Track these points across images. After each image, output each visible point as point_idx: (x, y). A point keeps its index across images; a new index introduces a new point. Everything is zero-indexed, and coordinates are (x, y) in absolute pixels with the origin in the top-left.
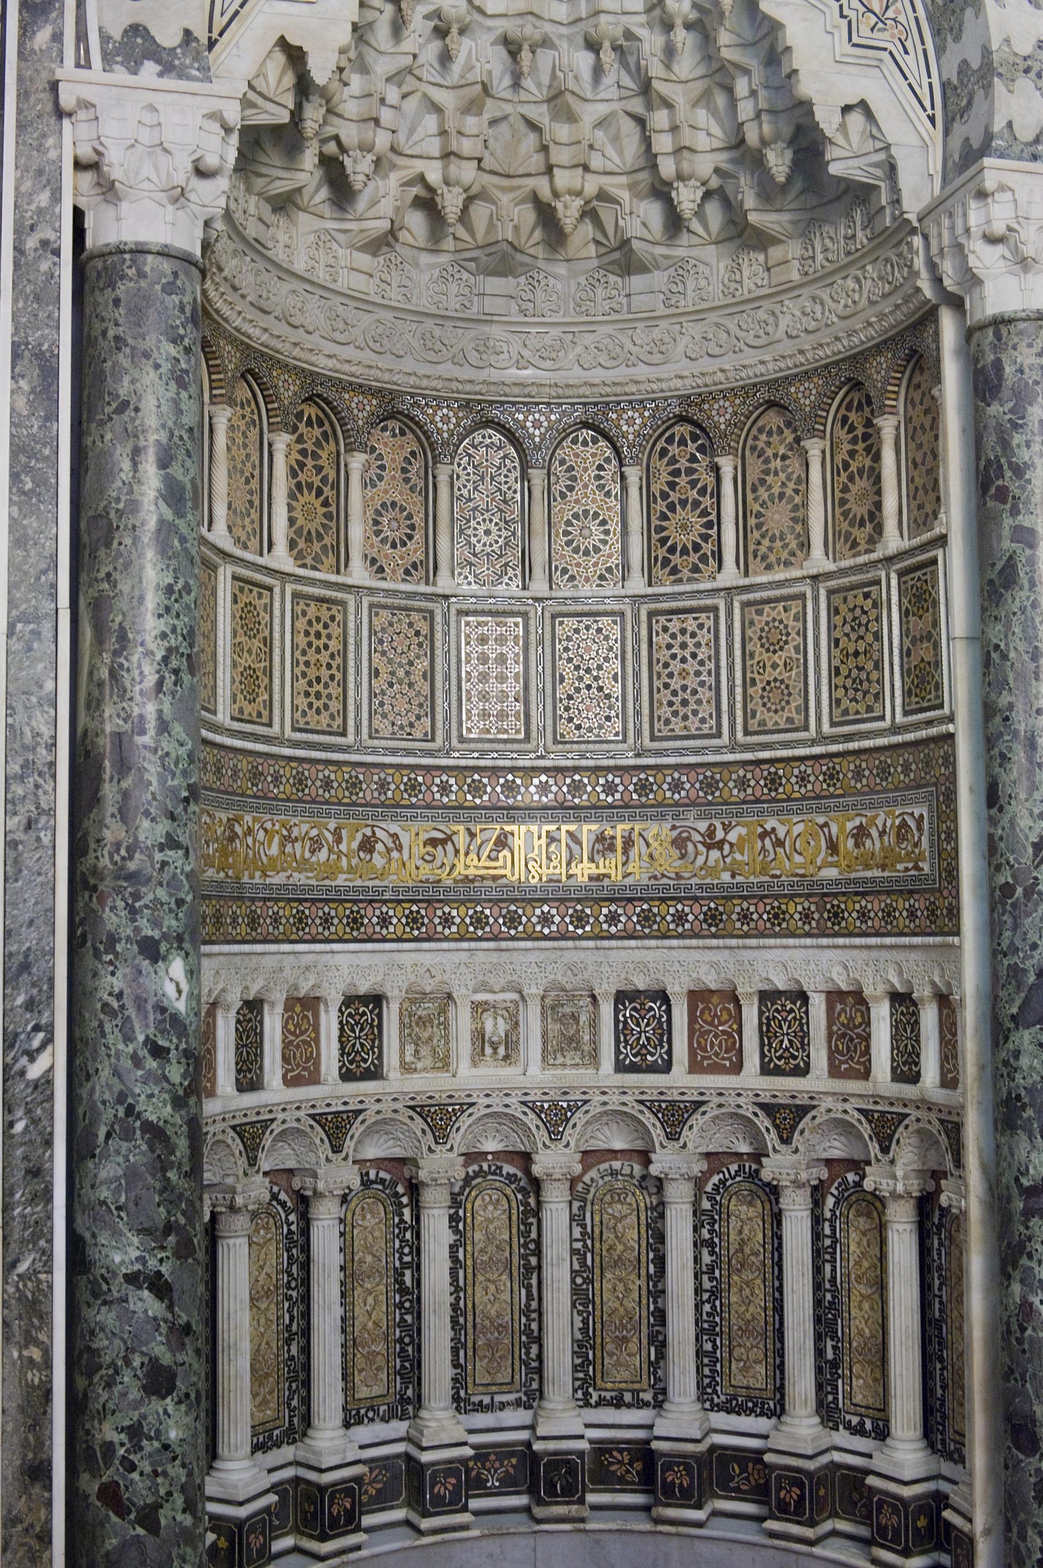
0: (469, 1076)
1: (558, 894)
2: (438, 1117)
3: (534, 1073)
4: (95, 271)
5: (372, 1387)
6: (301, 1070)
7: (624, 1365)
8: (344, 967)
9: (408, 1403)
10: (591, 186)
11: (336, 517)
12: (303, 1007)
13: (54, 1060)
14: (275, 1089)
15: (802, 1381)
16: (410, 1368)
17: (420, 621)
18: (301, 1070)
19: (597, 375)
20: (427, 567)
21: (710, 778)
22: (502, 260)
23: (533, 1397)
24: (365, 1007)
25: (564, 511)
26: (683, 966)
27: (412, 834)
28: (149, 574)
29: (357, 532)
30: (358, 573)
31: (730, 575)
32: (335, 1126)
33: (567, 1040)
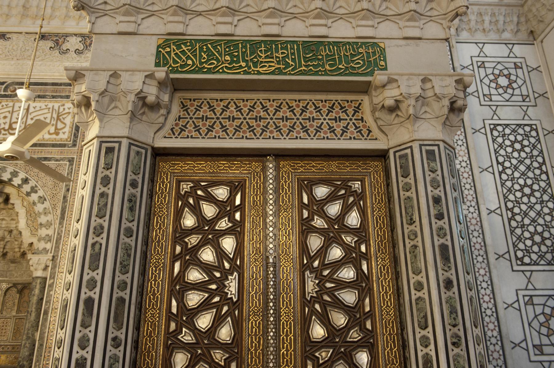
10: (22, 250)
19: (28, 278)
22: (13, 261)
25: (22, 301)
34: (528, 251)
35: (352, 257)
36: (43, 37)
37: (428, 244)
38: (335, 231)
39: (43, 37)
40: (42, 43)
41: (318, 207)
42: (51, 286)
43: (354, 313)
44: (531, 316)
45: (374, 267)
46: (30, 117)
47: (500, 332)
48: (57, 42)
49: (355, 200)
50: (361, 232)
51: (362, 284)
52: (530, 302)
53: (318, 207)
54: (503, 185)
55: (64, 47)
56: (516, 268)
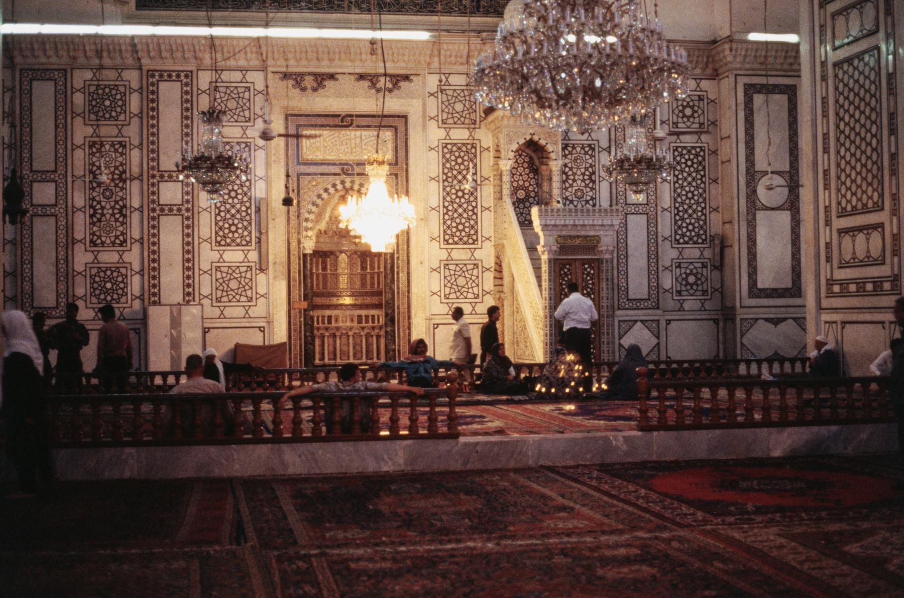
0: (341, 324)
1: (350, 305)
2: (338, 329)
3: (348, 324)
4: (305, 255)
5: (332, 357)
6: (323, 323)
7: (359, 356)
8: (328, 313)
9: (335, 359)
11: (326, 265)
12: (323, 317)
13: (302, 319)
14: (321, 325)
15: (375, 355)
16: (335, 355)
17: (336, 276)
18: (323, 323)
20: (336, 270)
21: (367, 293)
23: (348, 359)
24: (330, 317)
26: (363, 313)
27: (335, 299)
28: (309, 281)
29: (329, 267)
30: (329, 271)
31: (368, 271)
32: (327, 329)
33: (352, 320)
34: (683, 235)
35: (592, 279)
36: (361, 77)
37: (604, 277)
38: (589, 273)
39: (361, 77)
40: (361, 82)
41: (585, 269)
42: (398, 258)
43: (591, 289)
44: (678, 274)
45: (595, 281)
46: (363, 143)
47: (658, 284)
48: (371, 81)
49: (591, 268)
50: (593, 274)
51: (593, 284)
52: (679, 266)
53: (585, 269)
54: (675, 191)
55: (378, 86)
56: (674, 246)
